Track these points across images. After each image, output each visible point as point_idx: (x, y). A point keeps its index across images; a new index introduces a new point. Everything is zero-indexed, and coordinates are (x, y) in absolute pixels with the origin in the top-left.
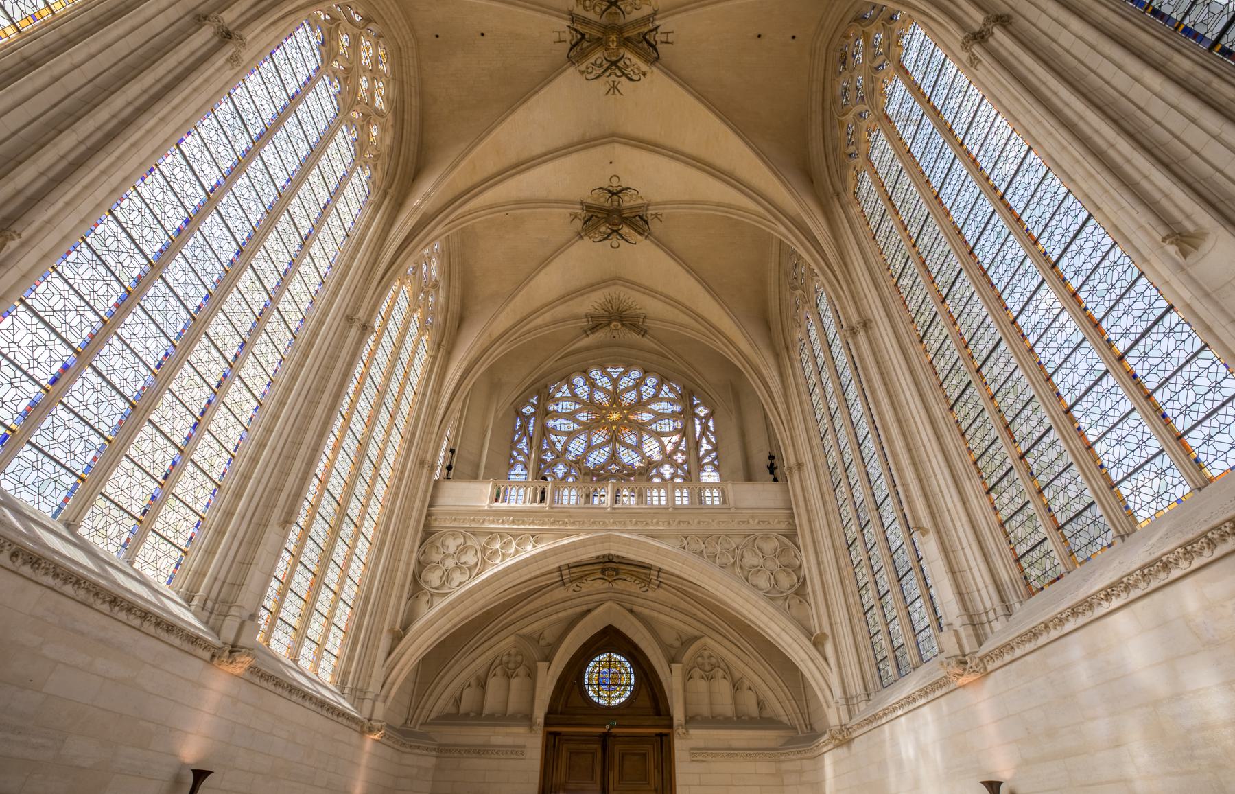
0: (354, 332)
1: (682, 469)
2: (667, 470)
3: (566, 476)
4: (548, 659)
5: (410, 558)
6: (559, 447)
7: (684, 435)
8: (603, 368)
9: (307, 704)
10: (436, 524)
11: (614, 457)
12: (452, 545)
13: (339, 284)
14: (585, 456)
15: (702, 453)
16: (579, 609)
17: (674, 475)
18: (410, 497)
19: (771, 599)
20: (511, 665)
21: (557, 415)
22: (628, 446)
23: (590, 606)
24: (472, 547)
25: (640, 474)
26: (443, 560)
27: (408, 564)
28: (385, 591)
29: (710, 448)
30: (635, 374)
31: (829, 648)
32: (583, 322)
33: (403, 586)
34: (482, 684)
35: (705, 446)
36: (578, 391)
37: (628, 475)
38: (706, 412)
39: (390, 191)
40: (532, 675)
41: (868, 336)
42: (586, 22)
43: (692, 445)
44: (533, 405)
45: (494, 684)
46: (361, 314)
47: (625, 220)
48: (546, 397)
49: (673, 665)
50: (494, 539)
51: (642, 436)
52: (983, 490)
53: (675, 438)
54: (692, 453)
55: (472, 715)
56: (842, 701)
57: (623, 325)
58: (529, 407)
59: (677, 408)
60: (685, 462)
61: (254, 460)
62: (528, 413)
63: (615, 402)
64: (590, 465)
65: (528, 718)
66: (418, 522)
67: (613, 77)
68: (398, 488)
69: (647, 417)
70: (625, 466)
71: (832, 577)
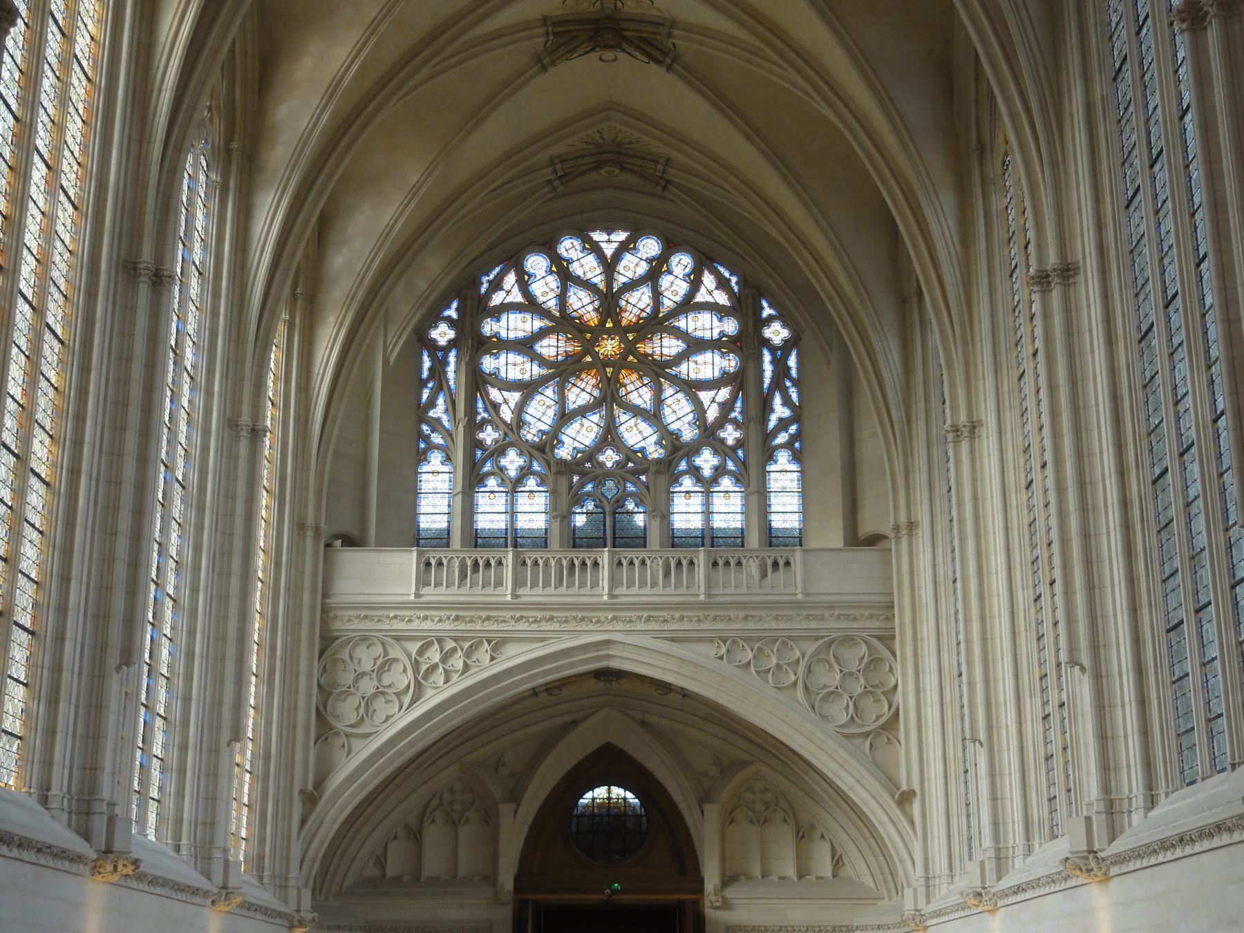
0: (244, 446)
1: (735, 459)
2: (707, 461)
3: (525, 472)
4: (515, 797)
5: (309, 686)
6: (507, 414)
9: (251, 914)
10: (337, 625)
11: (610, 436)
12: (367, 657)
13: (210, 371)
14: (552, 438)
15: (772, 424)
16: (559, 721)
17: (719, 471)
18: (295, 590)
19: (847, 736)
20: (457, 807)
22: (636, 411)
23: (576, 716)
24: (396, 660)
25: (657, 472)
26: (356, 680)
27: (309, 695)
28: (288, 743)
29: (785, 413)
30: (650, 247)
31: (916, 808)
32: (547, 173)
33: (307, 728)
34: (415, 835)
35: (780, 411)
36: (537, 289)
37: (636, 473)
38: (785, 333)
39: (235, 145)
40: (490, 819)
41: (972, 451)
43: (754, 411)
44: (451, 322)
45: (434, 835)
46: (245, 419)
47: (626, 39)
48: (477, 308)
49: (707, 807)
50: (428, 645)
52: (1040, 715)
53: (724, 394)
55: (405, 879)
56: (922, 881)
57: (623, 169)
58: (443, 327)
59: (731, 326)
60: (740, 443)
61: (189, 677)
62: (442, 342)
64: (564, 453)
65: (490, 879)
66: (312, 626)
68: (277, 580)
69: (670, 346)
70: (629, 454)
71: (932, 713)
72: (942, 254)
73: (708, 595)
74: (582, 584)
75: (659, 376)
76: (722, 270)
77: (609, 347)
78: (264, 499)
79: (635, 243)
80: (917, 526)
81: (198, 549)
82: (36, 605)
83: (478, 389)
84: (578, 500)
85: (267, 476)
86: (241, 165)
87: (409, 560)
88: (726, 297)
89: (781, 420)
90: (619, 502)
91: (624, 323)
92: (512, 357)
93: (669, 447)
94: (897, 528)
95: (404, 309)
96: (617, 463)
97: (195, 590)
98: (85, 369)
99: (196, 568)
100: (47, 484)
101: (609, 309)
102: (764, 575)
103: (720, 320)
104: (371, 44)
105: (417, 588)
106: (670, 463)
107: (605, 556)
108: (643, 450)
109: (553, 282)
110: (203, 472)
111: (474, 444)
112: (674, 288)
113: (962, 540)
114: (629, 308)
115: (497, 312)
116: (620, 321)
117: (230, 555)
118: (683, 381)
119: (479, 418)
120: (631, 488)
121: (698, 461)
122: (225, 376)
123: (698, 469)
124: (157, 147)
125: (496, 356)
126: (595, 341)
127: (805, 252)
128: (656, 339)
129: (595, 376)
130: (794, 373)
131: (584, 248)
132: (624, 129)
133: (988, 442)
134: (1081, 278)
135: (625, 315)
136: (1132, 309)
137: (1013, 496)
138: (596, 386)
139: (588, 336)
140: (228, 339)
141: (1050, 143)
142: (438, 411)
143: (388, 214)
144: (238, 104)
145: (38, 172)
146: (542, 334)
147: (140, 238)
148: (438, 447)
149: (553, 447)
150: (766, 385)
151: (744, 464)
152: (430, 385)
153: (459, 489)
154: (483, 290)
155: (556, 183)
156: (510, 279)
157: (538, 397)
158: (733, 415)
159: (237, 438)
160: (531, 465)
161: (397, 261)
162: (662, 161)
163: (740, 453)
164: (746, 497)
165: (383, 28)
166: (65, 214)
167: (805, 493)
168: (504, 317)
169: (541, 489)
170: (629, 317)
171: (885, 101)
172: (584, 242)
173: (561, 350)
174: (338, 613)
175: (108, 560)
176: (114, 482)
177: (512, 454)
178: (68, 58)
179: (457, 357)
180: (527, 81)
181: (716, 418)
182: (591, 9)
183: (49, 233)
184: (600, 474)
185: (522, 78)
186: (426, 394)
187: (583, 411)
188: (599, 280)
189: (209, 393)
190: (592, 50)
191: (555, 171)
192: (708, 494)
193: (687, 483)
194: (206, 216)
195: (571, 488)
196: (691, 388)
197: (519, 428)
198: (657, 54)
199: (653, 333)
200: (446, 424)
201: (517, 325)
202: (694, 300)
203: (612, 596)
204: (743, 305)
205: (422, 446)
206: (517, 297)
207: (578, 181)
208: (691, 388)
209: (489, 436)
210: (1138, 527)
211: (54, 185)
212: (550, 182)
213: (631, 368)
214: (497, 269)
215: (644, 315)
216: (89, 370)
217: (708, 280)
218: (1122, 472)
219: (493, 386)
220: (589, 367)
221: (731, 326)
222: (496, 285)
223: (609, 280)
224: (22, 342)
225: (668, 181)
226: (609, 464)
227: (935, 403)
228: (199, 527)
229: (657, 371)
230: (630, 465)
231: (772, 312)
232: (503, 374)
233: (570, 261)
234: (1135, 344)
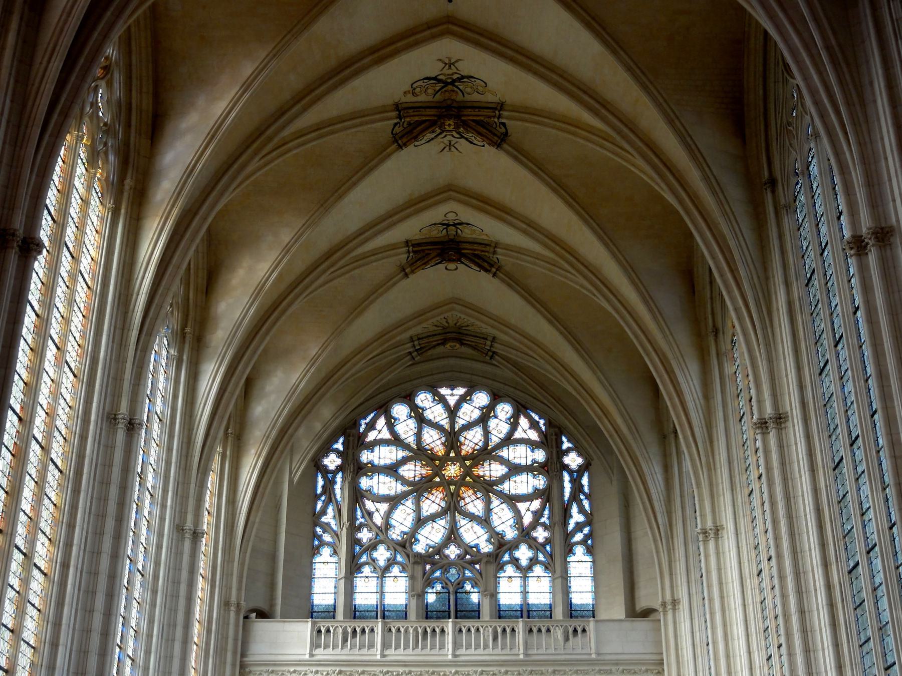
0: (187, 544)
1: (545, 553)
2: (524, 554)
3: (391, 563)
6: (378, 520)
7: (548, 500)
8: (433, 389)
11: (453, 536)
14: (411, 537)
15: (571, 527)
17: (533, 561)
18: (221, 651)
21: (375, 469)
22: (472, 517)
29: (581, 518)
30: (482, 399)
32: (408, 347)
35: (576, 517)
36: (400, 429)
37: (472, 563)
39: (188, 330)
42: (417, 108)
43: (558, 517)
44: (339, 453)
46: (189, 524)
47: (465, 256)
48: (356, 442)
51: (488, 502)
53: (536, 504)
54: (557, 529)
57: (462, 344)
58: (333, 456)
59: (540, 456)
60: (548, 541)
62: (332, 467)
63: (452, 448)
64: (420, 548)
67: (449, 138)
70: (467, 549)
72: (691, 405)
73: (526, 655)
74: (433, 647)
75: (488, 491)
76: (533, 415)
77: (452, 471)
78: (201, 583)
79: (471, 395)
80: (679, 603)
81: (151, 622)
82: (32, 665)
83: (357, 501)
84: (430, 583)
85: (203, 566)
86: (192, 342)
87: (303, 629)
88: (536, 435)
89: (577, 524)
90: (460, 585)
91: (463, 453)
92: (383, 478)
93: (496, 543)
94: (664, 604)
95: (305, 443)
96: (459, 556)
97: (148, 652)
98: (76, 491)
99: (150, 636)
100: (45, 575)
101: (452, 442)
102: (567, 639)
103: (532, 451)
104: (285, 261)
105: (311, 650)
106: (497, 556)
107: (449, 625)
108: (477, 546)
109: (412, 424)
110: (157, 564)
111: (354, 542)
112: (499, 428)
113: (712, 614)
114: (467, 442)
115: (371, 446)
116: (460, 452)
117: (175, 626)
118: (506, 495)
119: (358, 522)
120: (468, 574)
121: (517, 554)
122: (176, 493)
123: (517, 560)
124: (134, 333)
125: (371, 477)
126: (442, 467)
127: (592, 402)
128: (486, 464)
129: (442, 492)
130: (586, 489)
131: (434, 400)
132: (463, 316)
133: (729, 541)
134: (790, 424)
135: (463, 447)
136: (828, 446)
137: (748, 581)
138: (443, 499)
139: (437, 462)
140: (179, 467)
141: (764, 328)
142: (329, 518)
143: (294, 377)
144: (191, 301)
145: (51, 352)
146: (404, 461)
147: (120, 397)
148: (328, 544)
149: (411, 544)
150: (566, 498)
151: (551, 556)
152: (323, 498)
153: (343, 574)
154: (362, 430)
155: (415, 354)
156: (381, 422)
157: (401, 507)
158: (542, 520)
159: (183, 539)
160: (395, 557)
161: (301, 410)
162: (491, 339)
163: (548, 548)
164: (553, 580)
165: (294, 249)
166: (68, 380)
167: (596, 578)
168: (376, 449)
169: (403, 574)
170: (466, 449)
171: (647, 299)
172: (434, 395)
173: (418, 473)
174: (253, 669)
175: (86, 631)
176: (94, 573)
177: (382, 548)
178: (76, 273)
179: (342, 478)
180: (395, 284)
181: (531, 523)
182: (440, 235)
183: (56, 395)
184: (446, 565)
185: (391, 282)
186: (319, 505)
187: (433, 518)
188: (445, 423)
189: (163, 506)
190: (440, 263)
191: (414, 346)
192: (525, 578)
193: (510, 570)
194: (166, 379)
195: (424, 574)
196: (511, 500)
197: (387, 530)
198: (486, 265)
199: (484, 461)
200: (334, 527)
201: (386, 455)
202: (512, 437)
203: (454, 656)
204: (549, 441)
205: (316, 543)
206: (385, 434)
207: (430, 352)
208: (511, 500)
209: (365, 536)
210: (840, 606)
211: (61, 361)
212: (410, 353)
213: (468, 486)
214: (372, 415)
215: (477, 447)
216: (79, 492)
217: (524, 422)
218: (826, 565)
219: (368, 499)
220: (437, 485)
221: (540, 456)
222: (371, 426)
223: (452, 423)
224: (33, 472)
225: (494, 353)
226: (452, 557)
227: (689, 511)
228: (153, 605)
229: (487, 488)
230: (468, 557)
231: (570, 445)
232: (375, 491)
233: (424, 409)
234: (831, 472)
